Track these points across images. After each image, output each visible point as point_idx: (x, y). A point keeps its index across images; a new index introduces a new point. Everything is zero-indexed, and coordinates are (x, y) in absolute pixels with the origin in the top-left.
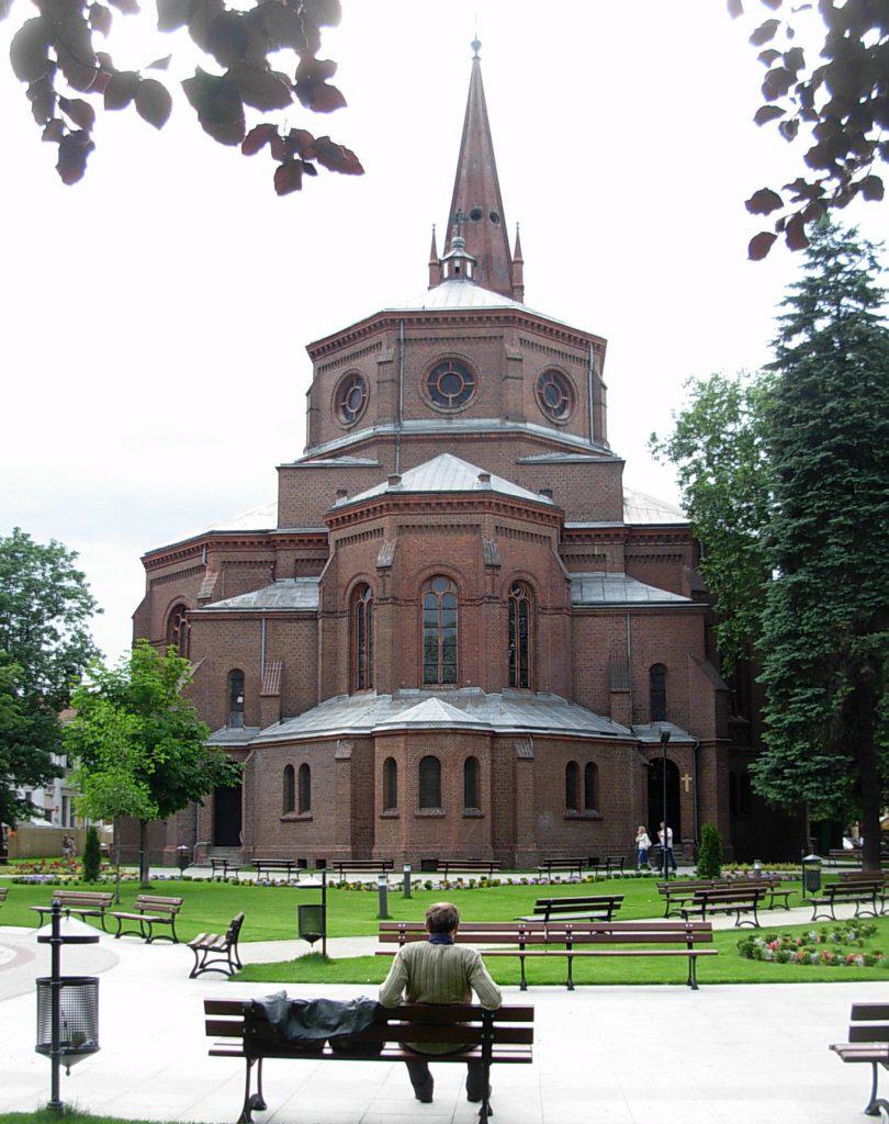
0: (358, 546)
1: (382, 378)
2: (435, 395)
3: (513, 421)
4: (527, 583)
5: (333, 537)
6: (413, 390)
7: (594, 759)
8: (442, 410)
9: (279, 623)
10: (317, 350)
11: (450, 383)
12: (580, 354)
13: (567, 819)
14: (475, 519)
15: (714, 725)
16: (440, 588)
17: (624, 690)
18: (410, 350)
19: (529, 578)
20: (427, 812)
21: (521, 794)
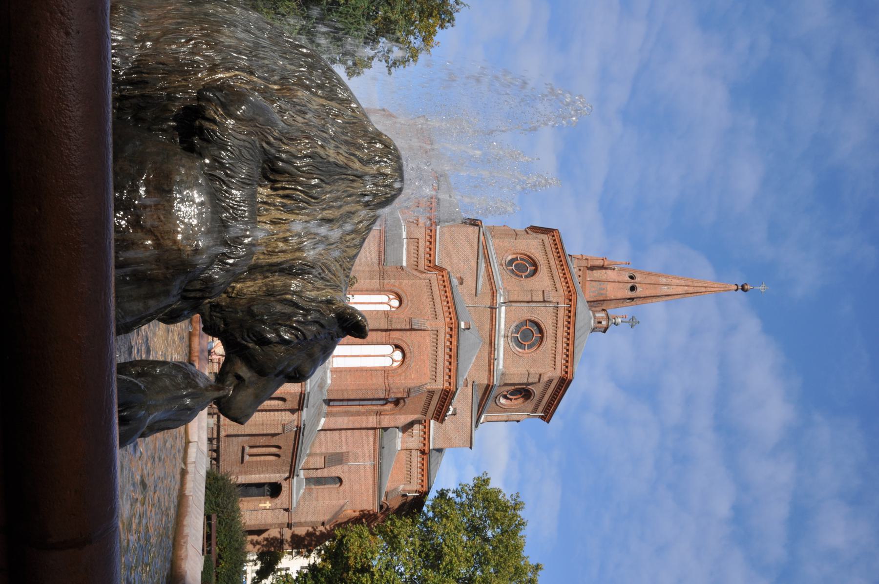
0: (426, 297)
1: (534, 293)
5: (433, 276)
6: (525, 312)
7: (283, 458)
11: (526, 335)
12: (541, 408)
18: (550, 310)
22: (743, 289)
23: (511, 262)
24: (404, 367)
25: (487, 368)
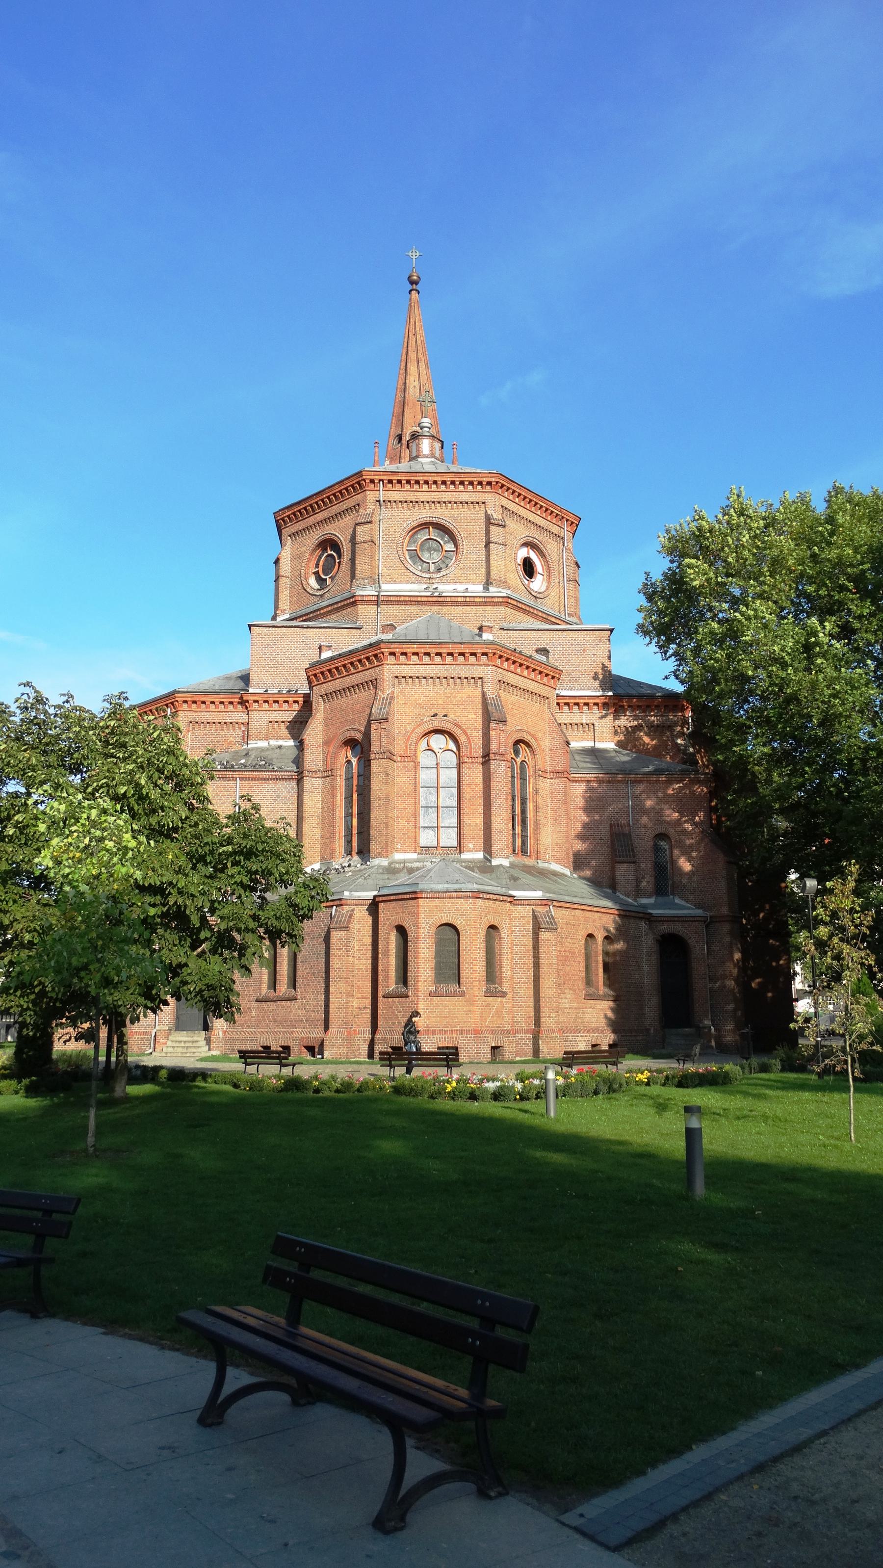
2: (415, 556)
3: (498, 586)
4: (528, 745)
8: (423, 575)
9: (252, 783)
10: (288, 519)
13: (589, 997)
14: (478, 671)
15: (726, 899)
16: (438, 742)
17: (629, 859)
19: (527, 738)
20: (443, 988)
21: (544, 970)
22: (416, 283)
23: (320, 580)
24: (457, 732)
25: (480, 608)
